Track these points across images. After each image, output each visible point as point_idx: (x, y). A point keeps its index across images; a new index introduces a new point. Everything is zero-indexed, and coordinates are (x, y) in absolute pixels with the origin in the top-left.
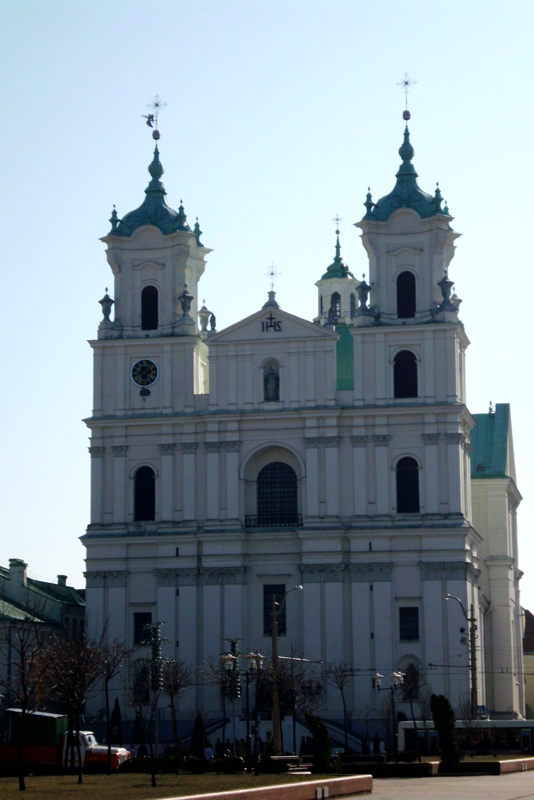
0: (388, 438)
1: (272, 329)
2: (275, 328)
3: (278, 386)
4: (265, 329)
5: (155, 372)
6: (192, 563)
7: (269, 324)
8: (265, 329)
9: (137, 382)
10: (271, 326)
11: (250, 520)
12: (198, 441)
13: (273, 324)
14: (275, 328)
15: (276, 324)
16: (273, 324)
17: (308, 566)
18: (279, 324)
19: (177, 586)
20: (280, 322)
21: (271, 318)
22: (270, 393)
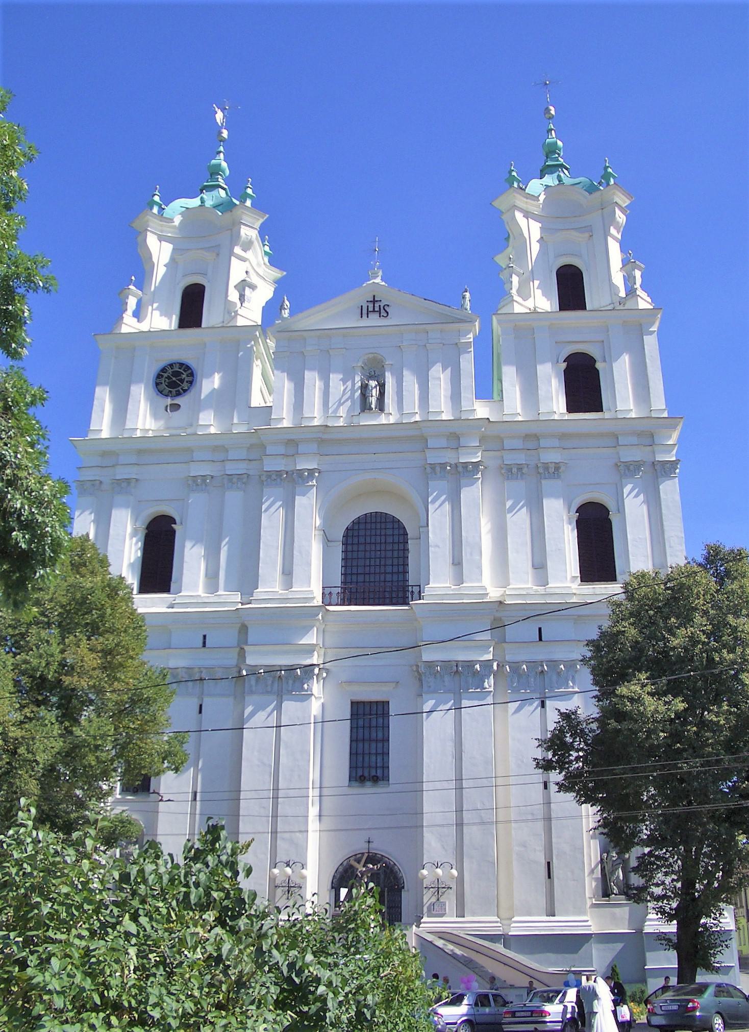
0: (563, 468)
1: (372, 316)
2: (380, 314)
3: (382, 394)
4: (365, 316)
5: (190, 379)
6: (230, 659)
7: (371, 309)
8: (365, 316)
9: (161, 392)
10: (374, 311)
11: (330, 593)
12: (251, 473)
13: (377, 309)
14: (380, 314)
15: (382, 308)
16: (377, 309)
17: (430, 665)
18: (386, 308)
19: (201, 696)
20: (388, 306)
21: (374, 301)
22: (373, 400)
